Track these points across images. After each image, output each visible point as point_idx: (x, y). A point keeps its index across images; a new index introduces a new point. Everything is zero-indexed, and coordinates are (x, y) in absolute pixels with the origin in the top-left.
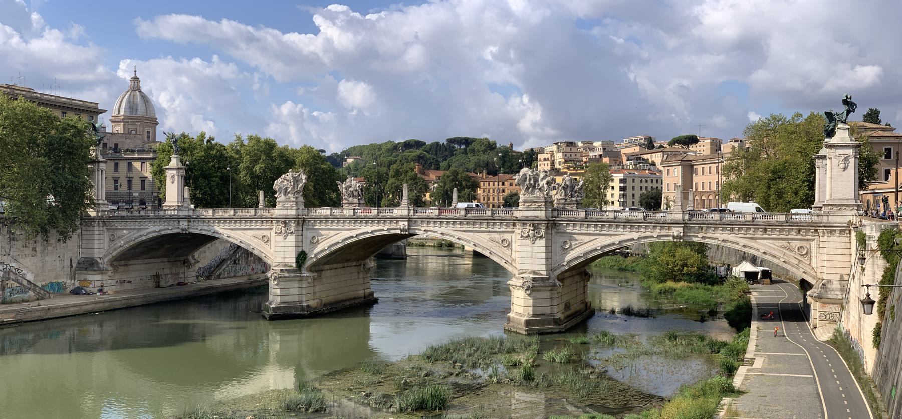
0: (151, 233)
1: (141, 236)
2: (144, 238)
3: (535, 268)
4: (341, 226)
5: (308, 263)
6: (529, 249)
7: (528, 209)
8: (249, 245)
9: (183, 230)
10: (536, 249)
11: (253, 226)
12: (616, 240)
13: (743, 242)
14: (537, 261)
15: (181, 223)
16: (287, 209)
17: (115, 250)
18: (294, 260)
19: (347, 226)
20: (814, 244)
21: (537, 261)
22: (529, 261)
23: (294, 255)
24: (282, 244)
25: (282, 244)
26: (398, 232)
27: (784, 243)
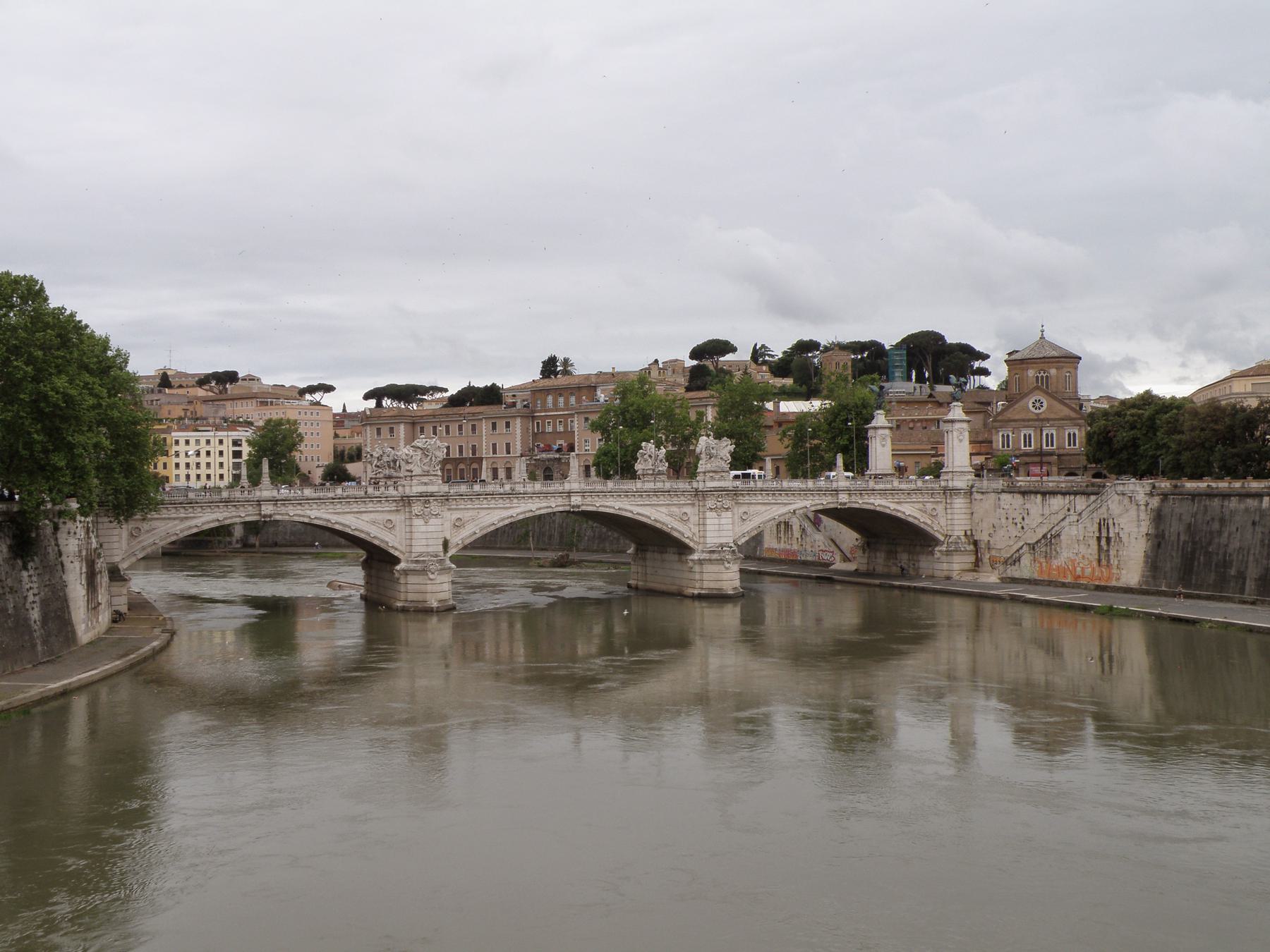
0: (209, 522)
1: (190, 528)
2: (195, 530)
3: (723, 541)
4: (493, 504)
5: (452, 552)
6: (716, 521)
7: (712, 479)
8: (368, 534)
9: (265, 516)
10: (723, 521)
11: (370, 506)
12: (792, 508)
13: (893, 506)
14: (724, 533)
15: (263, 508)
16: (426, 484)
17: (144, 548)
18: (441, 548)
19: (500, 503)
20: (940, 508)
21: (724, 533)
22: (716, 534)
23: (441, 542)
24: (423, 529)
25: (423, 529)
26: (567, 508)
27: (920, 505)
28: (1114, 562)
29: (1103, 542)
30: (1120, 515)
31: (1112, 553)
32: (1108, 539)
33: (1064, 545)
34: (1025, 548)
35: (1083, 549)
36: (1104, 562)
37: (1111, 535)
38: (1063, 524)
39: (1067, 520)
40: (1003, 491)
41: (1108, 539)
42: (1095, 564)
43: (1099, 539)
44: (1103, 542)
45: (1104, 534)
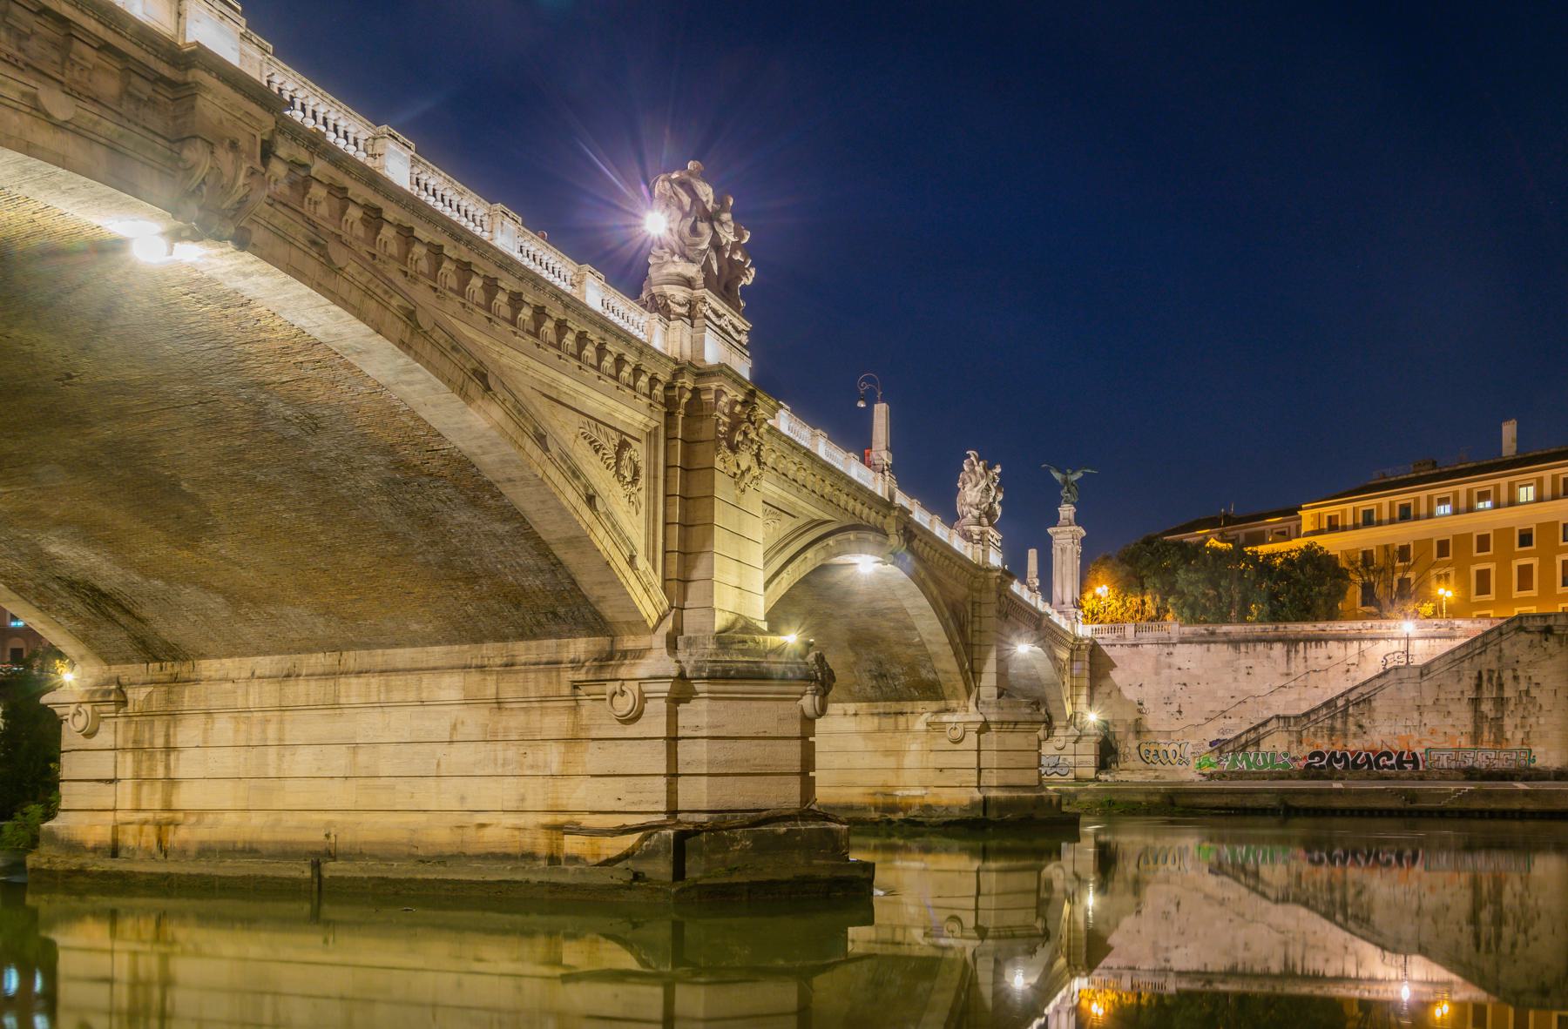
28: (1513, 734)
29: (1487, 707)
30: (1530, 664)
31: (1508, 723)
32: (1500, 702)
33: (1379, 716)
34: (1273, 725)
35: (1431, 719)
36: (1487, 735)
37: (1509, 692)
38: (1378, 683)
39: (1391, 676)
40: (1183, 641)
41: (1500, 702)
42: (1464, 742)
43: (1476, 702)
44: (1487, 707)
45: (1489, 692)
